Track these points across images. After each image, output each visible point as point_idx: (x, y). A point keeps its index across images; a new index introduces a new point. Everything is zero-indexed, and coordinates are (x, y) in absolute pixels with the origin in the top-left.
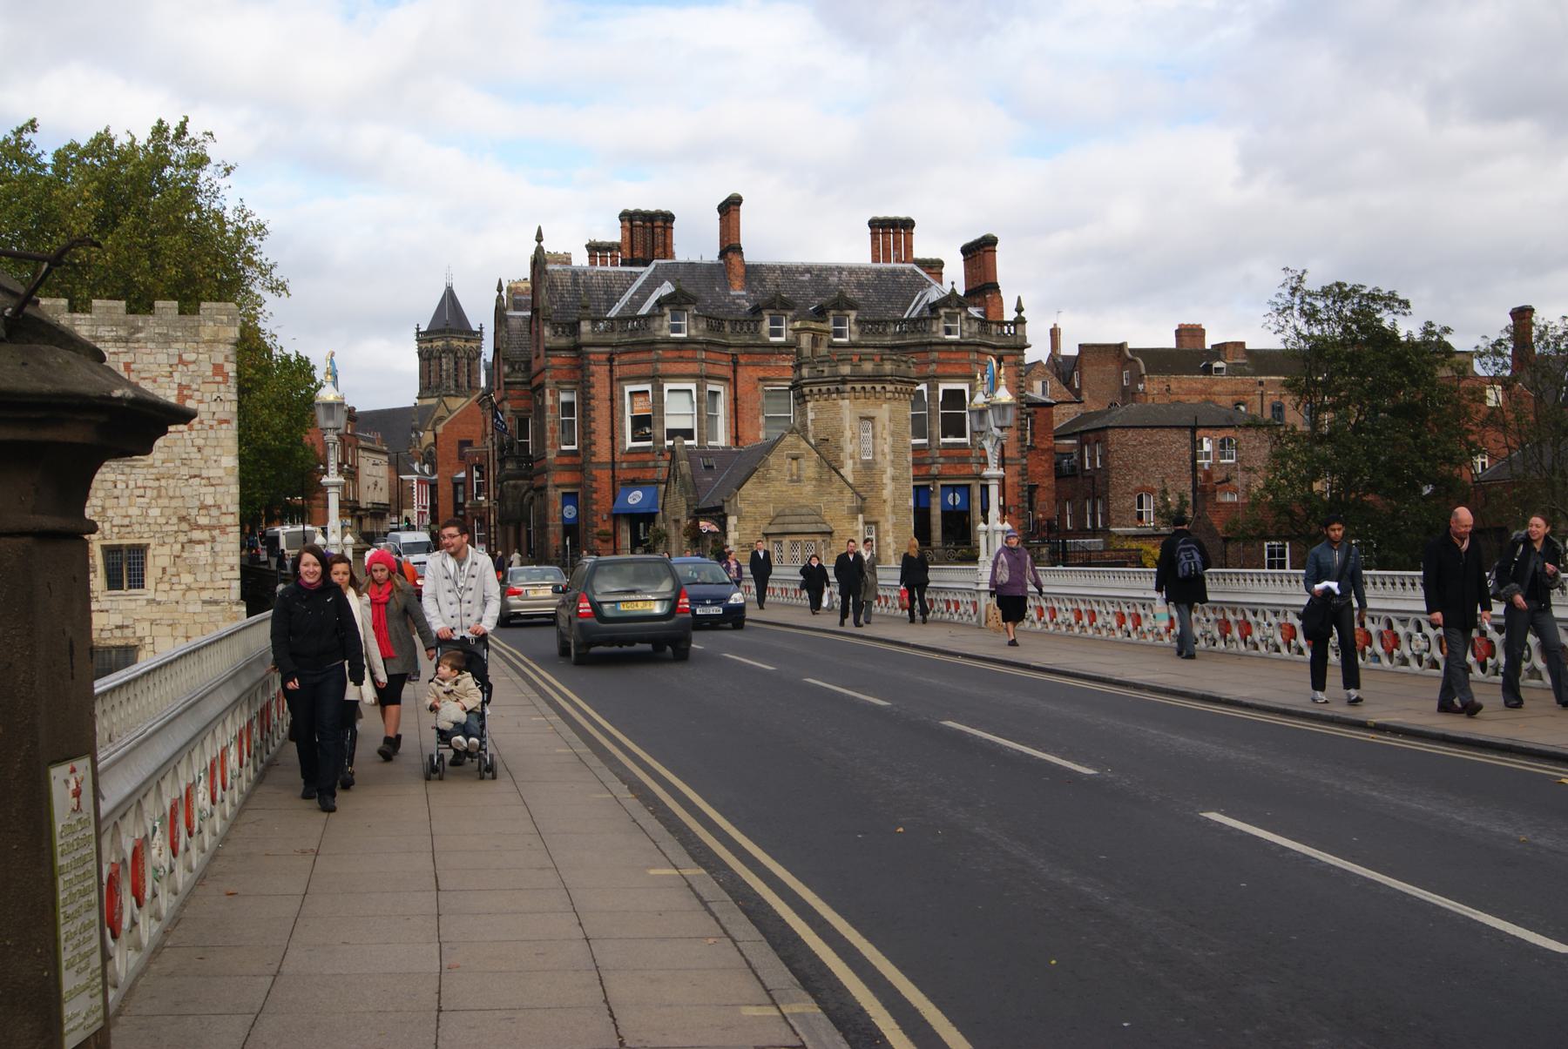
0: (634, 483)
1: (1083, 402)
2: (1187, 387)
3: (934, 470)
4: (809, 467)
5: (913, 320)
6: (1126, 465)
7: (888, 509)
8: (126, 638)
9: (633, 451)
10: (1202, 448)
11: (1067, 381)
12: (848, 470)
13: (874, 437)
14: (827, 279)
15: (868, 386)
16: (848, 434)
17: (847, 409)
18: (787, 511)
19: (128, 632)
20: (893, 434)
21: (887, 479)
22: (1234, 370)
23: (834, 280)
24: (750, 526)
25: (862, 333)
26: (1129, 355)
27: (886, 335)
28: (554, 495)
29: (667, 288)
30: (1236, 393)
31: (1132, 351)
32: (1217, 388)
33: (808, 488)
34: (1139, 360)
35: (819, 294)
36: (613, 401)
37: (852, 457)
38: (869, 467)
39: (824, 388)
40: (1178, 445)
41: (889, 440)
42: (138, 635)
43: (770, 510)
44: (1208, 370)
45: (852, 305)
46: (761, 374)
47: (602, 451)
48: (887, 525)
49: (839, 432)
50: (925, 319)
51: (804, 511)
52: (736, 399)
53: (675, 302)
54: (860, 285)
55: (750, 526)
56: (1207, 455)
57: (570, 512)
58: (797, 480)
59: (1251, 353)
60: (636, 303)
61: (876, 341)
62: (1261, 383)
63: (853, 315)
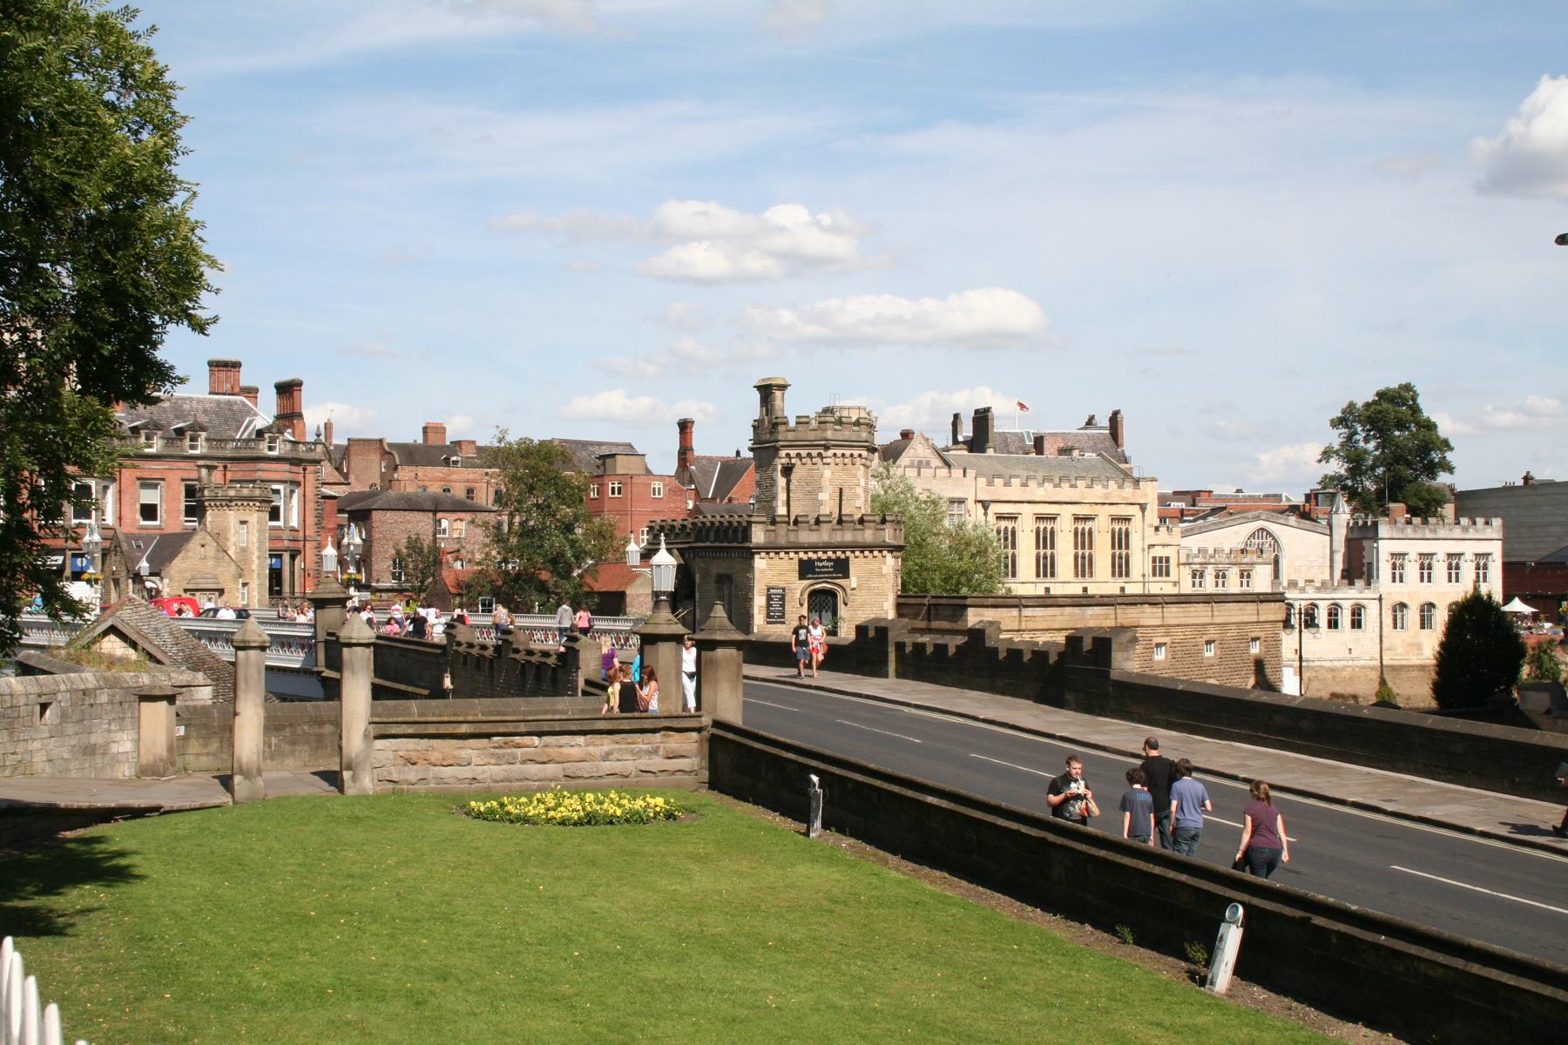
1: (349, 484)
2: (431, 480)
4: (211, 549)
5: (244, 440)
6: (385, 537)
7: (255, 576)
10: (440, 526)
11: (338, 469)
13: (248, 533)
14: (181, 406)
15: (245, 503)
16: (232, 531)
17: (232, 516)
18: (198, 576)
20: (259, 531)
21: (254, 557)
22: (468, 464)
23: (186, 407)
24: (176, 584)
25: (210, 447)
26: (387, 448)
27: (226, 449)
30: (468, 481)
31: (389, 445)
32: (454, 477)
33: (211, 563)
34: (394, 452)
35: (177, 417)
37: (235, 545)
38: (244, 551)
39: (218, 504)
40: (423, 524)
41: (257, 535)
43: (188, 575)
44: (447, 462)
45: (203, 429)
46: (139, 474)
48: (254, 584)
49: (226, 529)
50: (253, 440)
51: (208, 576)
52: (120, 492)
54: (205, 411)
55: (176, 584)
56: (444, 530)
59: (480, 450)
61: (220, 453)
62: (487, 474)
63: (204, 435)
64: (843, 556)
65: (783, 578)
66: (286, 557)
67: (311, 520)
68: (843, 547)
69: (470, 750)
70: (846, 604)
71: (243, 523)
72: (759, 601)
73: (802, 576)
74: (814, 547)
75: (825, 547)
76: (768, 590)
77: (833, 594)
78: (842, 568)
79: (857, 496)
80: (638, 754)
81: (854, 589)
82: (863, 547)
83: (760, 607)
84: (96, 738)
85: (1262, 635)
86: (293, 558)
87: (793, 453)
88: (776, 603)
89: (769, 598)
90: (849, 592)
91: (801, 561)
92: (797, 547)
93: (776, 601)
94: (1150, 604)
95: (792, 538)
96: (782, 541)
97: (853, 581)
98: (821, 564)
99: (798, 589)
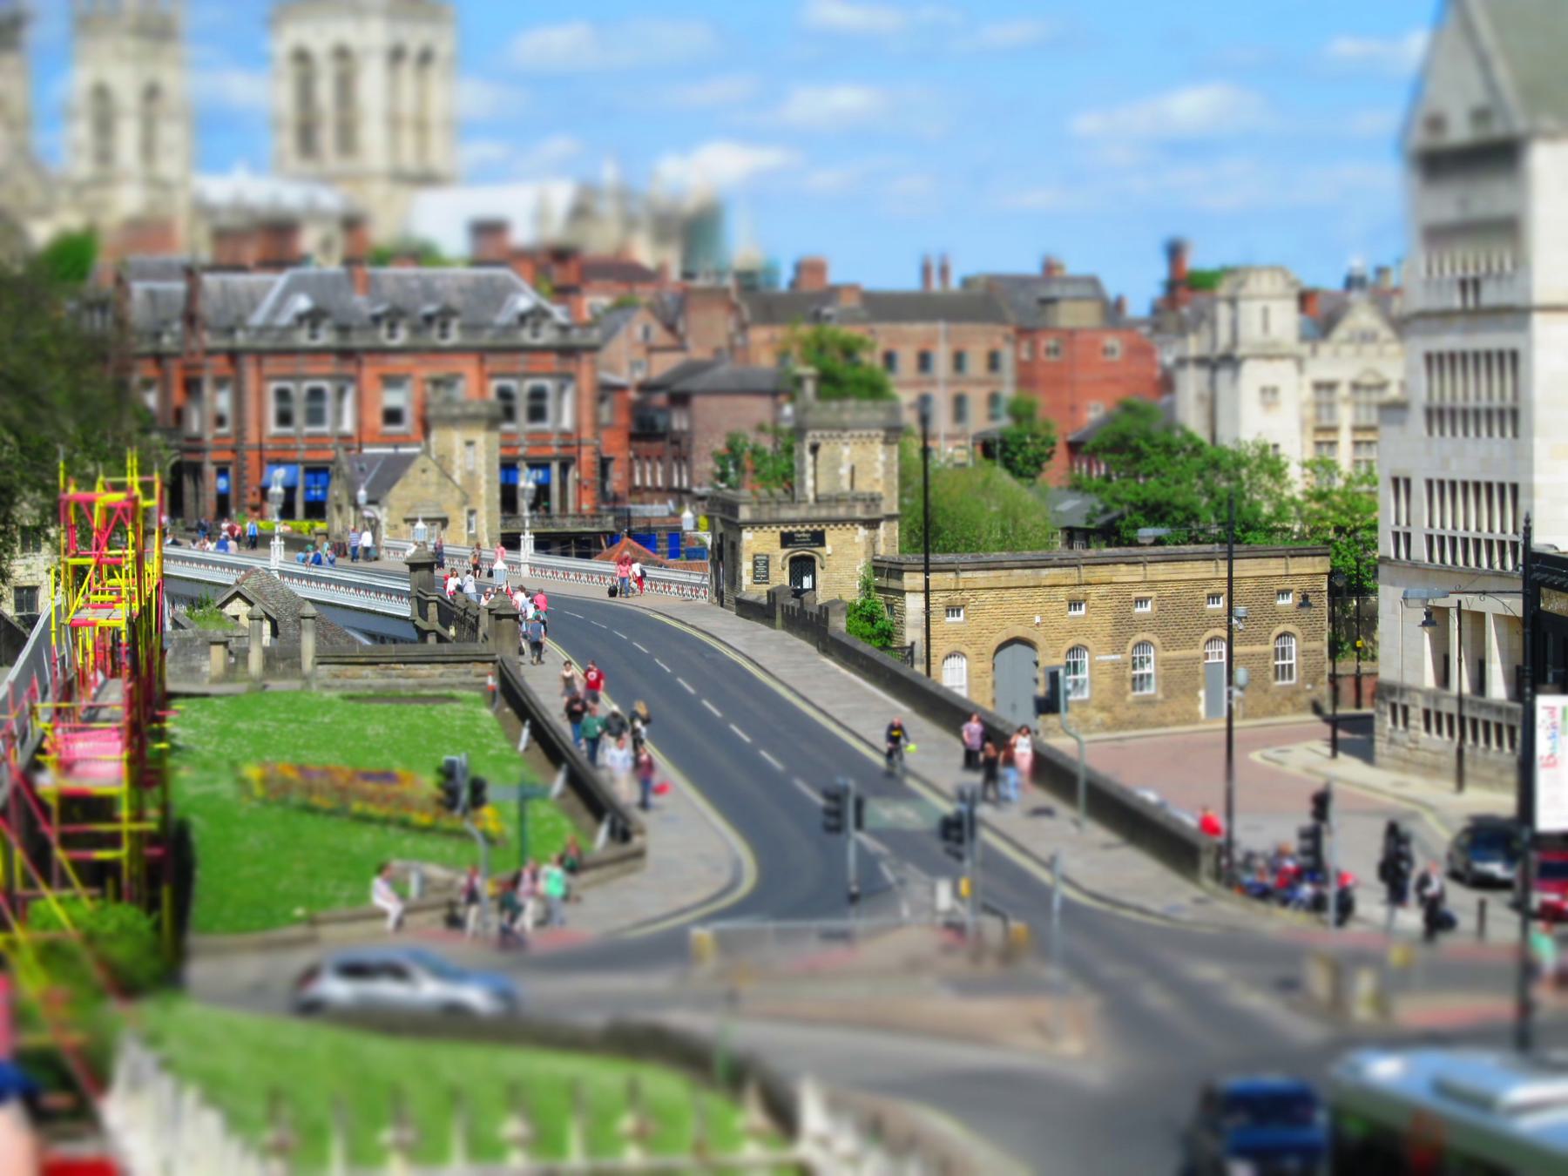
0: (279, 463)
3: (521, 451)
4: (433, 476)
7: (483, 501)
8: (33, 581)
9: (277, 437)
11: (671, 328)
12: (457, 477)
16: (457, 452)
19: (34, 578)
28: (210, 469)
29: (303, 303)
33: (432, 490)
36: (260, 395)
37: (460, 467)
38: (471, 475)
42: (40, 579)
43: (408, 503)
47: (252, 437)
48: (482, 511)
49: (451, 451)
53: (313, 318)
54: (462, 290)
57: (222, 484)
58: (425, 485)
60: (276, 311)
64: (819, 529)
65: (767, 547)
66: (555, 467)
67: (587, 420)
68: (819, 521)
69: (367, 671)
70: (822, 568)
71: (470, 443)
72: (746, 566)
73: (784, 544)
74: (793, 522)
75: (803, 522)
76: (755, 556)
77: (811, 560)
78: (819, 538)
79: (875, 470)
80: (459, 674)
81: (829, 555)
82: (837, 522)
83: (747, 570)
84: (194, 663)
85: (1296, 587)
86: (564, 468)
87: (818, 433)
88: (761, 568)
89: (755, 563)
90: (825, 558)
91: (783, 535)
92: (779, 523)
93: (762, 565)
94: (1128, 564)
95: (774, 515)
96: (765, 517)
97: (828, 549)
98: (799, 536)
99: (780, 556)
